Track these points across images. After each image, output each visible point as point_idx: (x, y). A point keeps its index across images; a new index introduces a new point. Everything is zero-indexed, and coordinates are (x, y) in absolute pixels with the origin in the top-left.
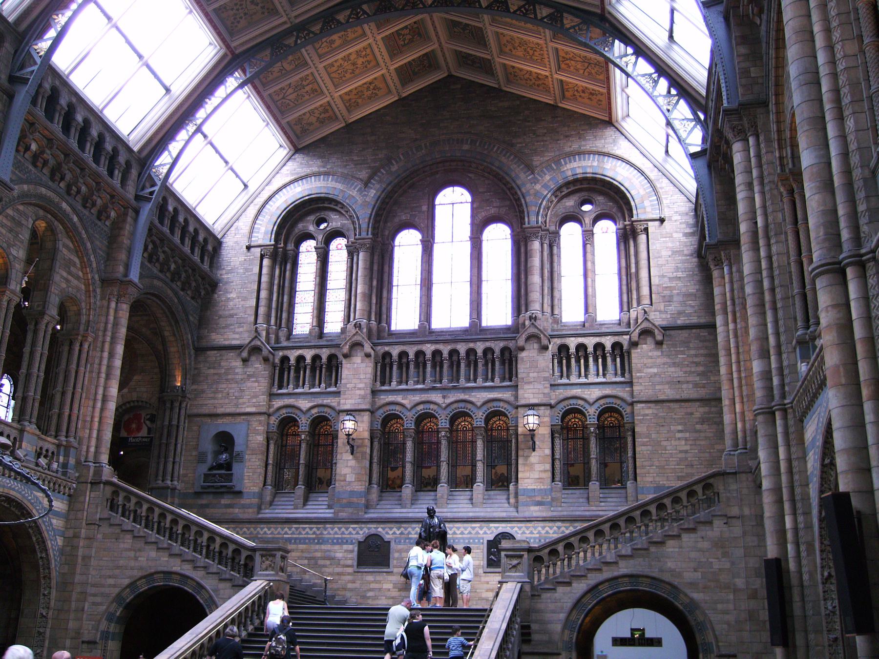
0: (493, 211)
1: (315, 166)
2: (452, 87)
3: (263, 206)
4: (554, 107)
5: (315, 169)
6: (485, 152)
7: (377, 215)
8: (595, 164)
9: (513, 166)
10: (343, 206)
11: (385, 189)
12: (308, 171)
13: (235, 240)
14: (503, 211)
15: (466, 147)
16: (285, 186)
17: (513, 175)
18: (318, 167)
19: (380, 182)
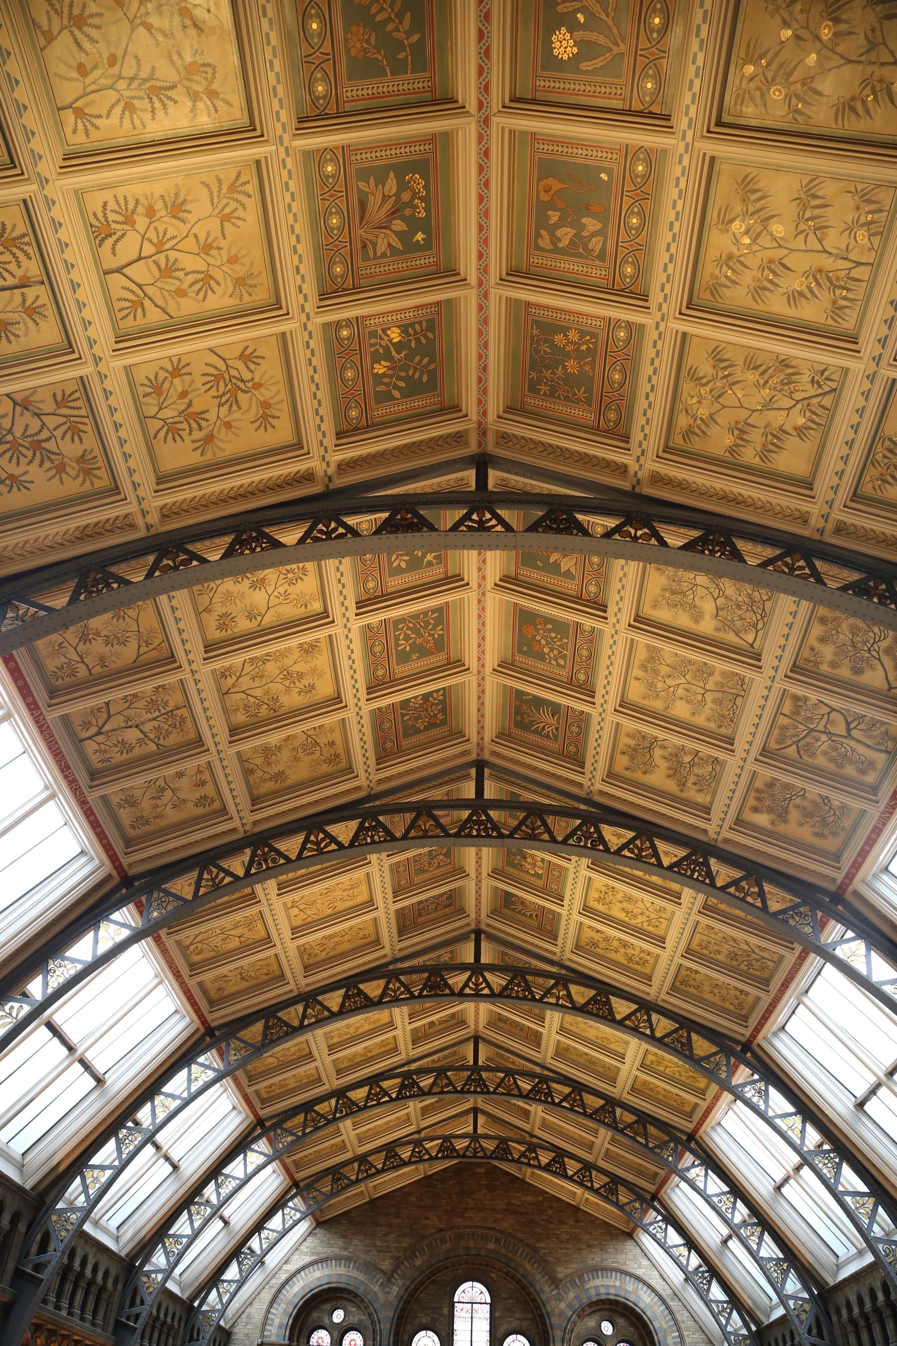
0: (515, 1324)
1: (336, 1247)
2: (478, 1170)
3: (279, 1291)
4: (576, 1209)
5: (336, 1250)
6: (510, 1255)
7: (400, 1317)
8: (618, 1284)
9: (538, 1276)
10: (362, 1301)
11: (408, 1287)
12: (327, 1251)
13: (246, 1331)
14: (526, 1324)
15: (491, 1246)
16: (303, 1268)
17: (538, 1288)
18: (341, 1248)
19: (403, 1278)
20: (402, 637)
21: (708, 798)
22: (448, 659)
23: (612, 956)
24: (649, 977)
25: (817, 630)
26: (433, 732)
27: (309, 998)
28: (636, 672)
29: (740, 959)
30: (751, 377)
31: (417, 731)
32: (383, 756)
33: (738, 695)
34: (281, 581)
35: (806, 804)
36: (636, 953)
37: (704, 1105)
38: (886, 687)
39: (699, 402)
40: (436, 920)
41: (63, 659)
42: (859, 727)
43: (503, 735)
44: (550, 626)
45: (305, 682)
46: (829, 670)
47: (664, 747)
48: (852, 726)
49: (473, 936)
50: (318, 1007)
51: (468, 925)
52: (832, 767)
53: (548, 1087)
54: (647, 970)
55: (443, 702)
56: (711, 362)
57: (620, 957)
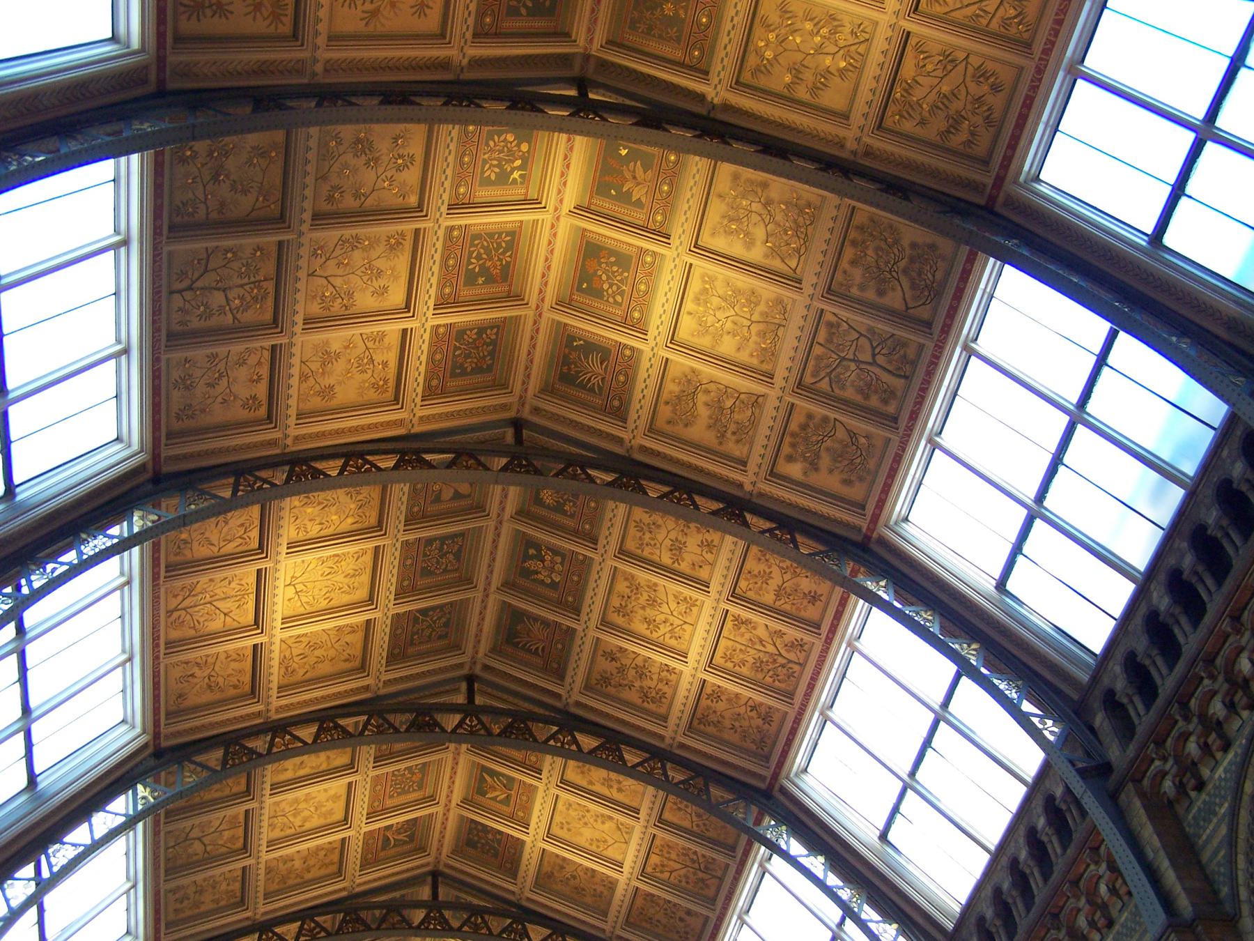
20: (474, 255)
21: (745, 449)
22: (509, 291)
23: (627, 695)
24: (665, 718)
25: (849, 253)
26: (478, 379)
27: (279, 728)
28: (689, 305)
29: (766, 668)
30: (808, 26)
31: (464, 373)
32: (430, 393)
33: (780, 325)
34: (391, 165)
35: (836, 446)
36: (652, 684)
37: (713, 917)
38: (904, 308)
39: (766, 45)
40: (428, 653)
41: (190, 195)
42: (883, 352)
43: (548, 390)
44: (613, 259)
45: (382, 282)
46: (858, 293)
47: (707, 392)
48: (877, 350)
49: (464, 686)
50: (288, 737)
51: (461, 665)
52: (858, 398)
53: (524, 927)
54: (663, 711)
55: (494, 343)
56: (778, 13)
57: (633, 697)
